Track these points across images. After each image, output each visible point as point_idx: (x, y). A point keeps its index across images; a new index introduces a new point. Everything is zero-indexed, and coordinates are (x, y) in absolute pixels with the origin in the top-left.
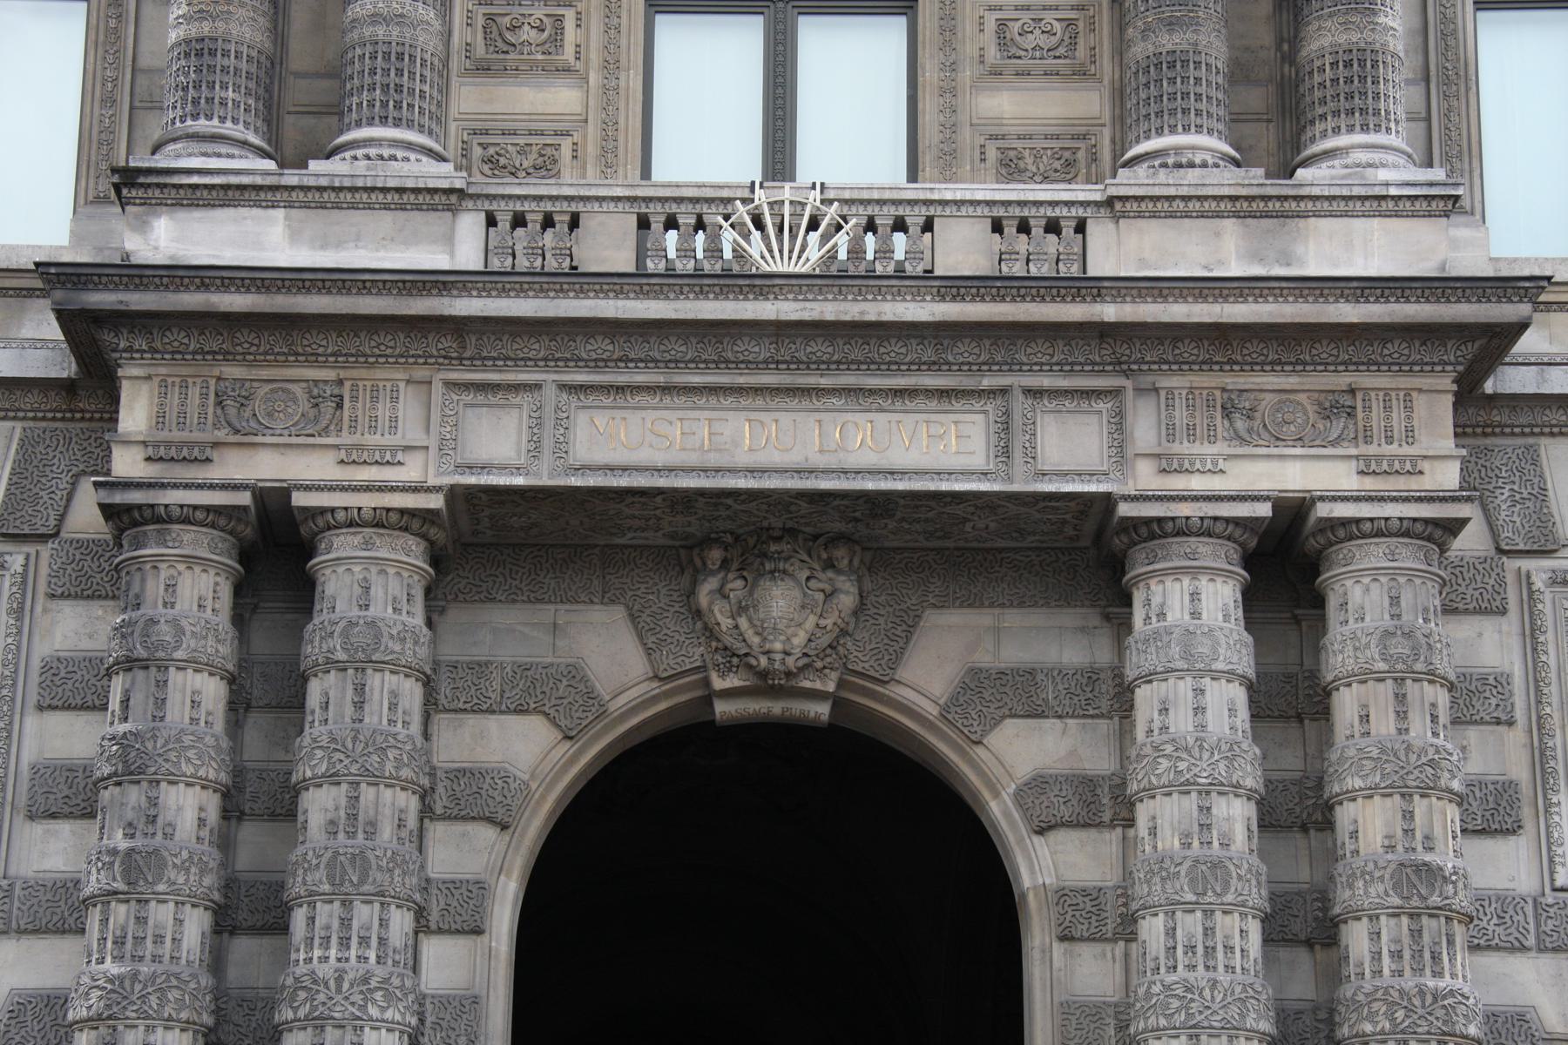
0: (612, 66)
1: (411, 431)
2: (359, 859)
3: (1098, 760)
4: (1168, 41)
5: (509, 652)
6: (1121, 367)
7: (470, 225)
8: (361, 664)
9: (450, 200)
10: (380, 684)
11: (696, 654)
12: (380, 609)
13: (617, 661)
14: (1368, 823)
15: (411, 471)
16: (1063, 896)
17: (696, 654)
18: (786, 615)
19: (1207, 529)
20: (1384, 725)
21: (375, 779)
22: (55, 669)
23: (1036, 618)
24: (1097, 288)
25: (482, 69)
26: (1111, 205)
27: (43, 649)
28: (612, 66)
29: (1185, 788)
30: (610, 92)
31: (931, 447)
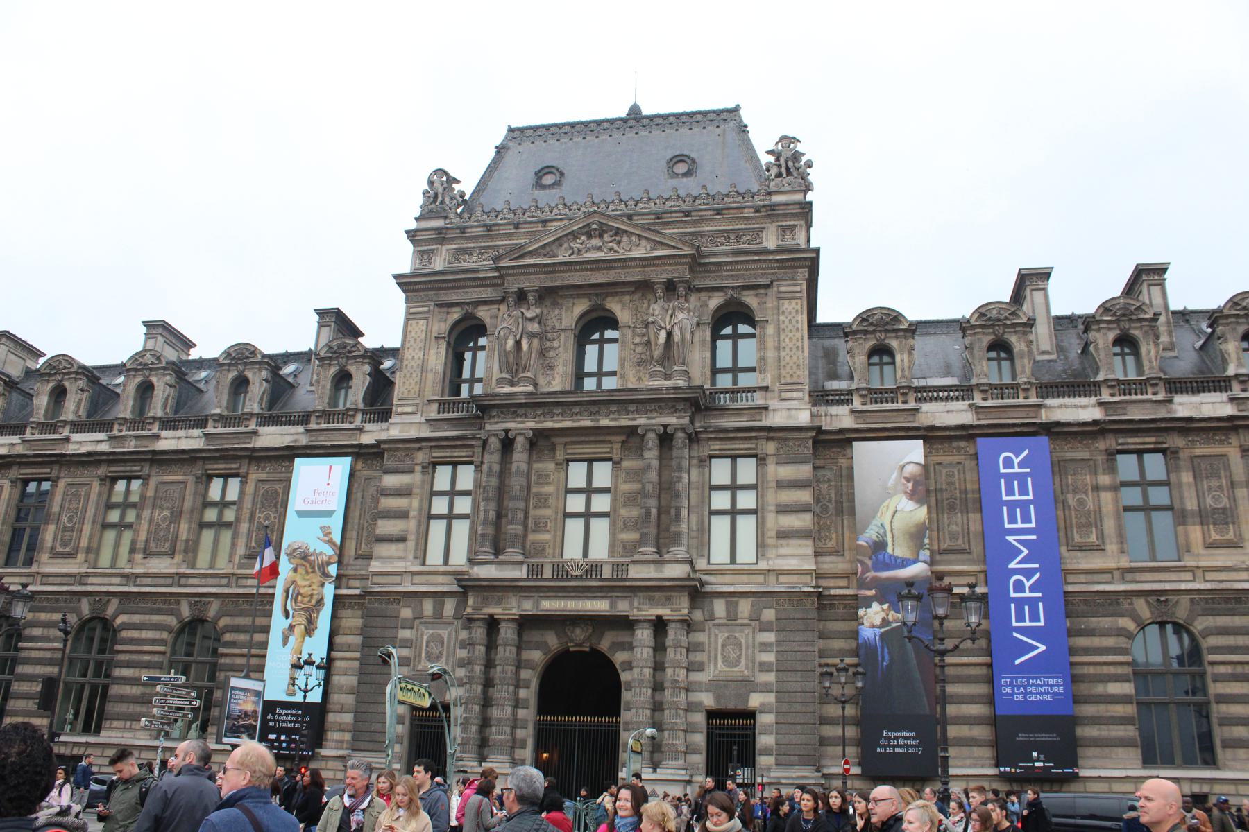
0: (555, 531)
1: (514, 604)
7: (525, 567)
8: (505, 645)
9: (522, 563)
12: (508, 635)
13: (553, 641)
15: (514, 611)
18: (579, 634)
19: (645, 621)
22: (463, 641)
24: (627, 580)
25: (534, 531)
26: (633, 562)
28: (555, 531)
30: (555, 536)
31: (599, 606)
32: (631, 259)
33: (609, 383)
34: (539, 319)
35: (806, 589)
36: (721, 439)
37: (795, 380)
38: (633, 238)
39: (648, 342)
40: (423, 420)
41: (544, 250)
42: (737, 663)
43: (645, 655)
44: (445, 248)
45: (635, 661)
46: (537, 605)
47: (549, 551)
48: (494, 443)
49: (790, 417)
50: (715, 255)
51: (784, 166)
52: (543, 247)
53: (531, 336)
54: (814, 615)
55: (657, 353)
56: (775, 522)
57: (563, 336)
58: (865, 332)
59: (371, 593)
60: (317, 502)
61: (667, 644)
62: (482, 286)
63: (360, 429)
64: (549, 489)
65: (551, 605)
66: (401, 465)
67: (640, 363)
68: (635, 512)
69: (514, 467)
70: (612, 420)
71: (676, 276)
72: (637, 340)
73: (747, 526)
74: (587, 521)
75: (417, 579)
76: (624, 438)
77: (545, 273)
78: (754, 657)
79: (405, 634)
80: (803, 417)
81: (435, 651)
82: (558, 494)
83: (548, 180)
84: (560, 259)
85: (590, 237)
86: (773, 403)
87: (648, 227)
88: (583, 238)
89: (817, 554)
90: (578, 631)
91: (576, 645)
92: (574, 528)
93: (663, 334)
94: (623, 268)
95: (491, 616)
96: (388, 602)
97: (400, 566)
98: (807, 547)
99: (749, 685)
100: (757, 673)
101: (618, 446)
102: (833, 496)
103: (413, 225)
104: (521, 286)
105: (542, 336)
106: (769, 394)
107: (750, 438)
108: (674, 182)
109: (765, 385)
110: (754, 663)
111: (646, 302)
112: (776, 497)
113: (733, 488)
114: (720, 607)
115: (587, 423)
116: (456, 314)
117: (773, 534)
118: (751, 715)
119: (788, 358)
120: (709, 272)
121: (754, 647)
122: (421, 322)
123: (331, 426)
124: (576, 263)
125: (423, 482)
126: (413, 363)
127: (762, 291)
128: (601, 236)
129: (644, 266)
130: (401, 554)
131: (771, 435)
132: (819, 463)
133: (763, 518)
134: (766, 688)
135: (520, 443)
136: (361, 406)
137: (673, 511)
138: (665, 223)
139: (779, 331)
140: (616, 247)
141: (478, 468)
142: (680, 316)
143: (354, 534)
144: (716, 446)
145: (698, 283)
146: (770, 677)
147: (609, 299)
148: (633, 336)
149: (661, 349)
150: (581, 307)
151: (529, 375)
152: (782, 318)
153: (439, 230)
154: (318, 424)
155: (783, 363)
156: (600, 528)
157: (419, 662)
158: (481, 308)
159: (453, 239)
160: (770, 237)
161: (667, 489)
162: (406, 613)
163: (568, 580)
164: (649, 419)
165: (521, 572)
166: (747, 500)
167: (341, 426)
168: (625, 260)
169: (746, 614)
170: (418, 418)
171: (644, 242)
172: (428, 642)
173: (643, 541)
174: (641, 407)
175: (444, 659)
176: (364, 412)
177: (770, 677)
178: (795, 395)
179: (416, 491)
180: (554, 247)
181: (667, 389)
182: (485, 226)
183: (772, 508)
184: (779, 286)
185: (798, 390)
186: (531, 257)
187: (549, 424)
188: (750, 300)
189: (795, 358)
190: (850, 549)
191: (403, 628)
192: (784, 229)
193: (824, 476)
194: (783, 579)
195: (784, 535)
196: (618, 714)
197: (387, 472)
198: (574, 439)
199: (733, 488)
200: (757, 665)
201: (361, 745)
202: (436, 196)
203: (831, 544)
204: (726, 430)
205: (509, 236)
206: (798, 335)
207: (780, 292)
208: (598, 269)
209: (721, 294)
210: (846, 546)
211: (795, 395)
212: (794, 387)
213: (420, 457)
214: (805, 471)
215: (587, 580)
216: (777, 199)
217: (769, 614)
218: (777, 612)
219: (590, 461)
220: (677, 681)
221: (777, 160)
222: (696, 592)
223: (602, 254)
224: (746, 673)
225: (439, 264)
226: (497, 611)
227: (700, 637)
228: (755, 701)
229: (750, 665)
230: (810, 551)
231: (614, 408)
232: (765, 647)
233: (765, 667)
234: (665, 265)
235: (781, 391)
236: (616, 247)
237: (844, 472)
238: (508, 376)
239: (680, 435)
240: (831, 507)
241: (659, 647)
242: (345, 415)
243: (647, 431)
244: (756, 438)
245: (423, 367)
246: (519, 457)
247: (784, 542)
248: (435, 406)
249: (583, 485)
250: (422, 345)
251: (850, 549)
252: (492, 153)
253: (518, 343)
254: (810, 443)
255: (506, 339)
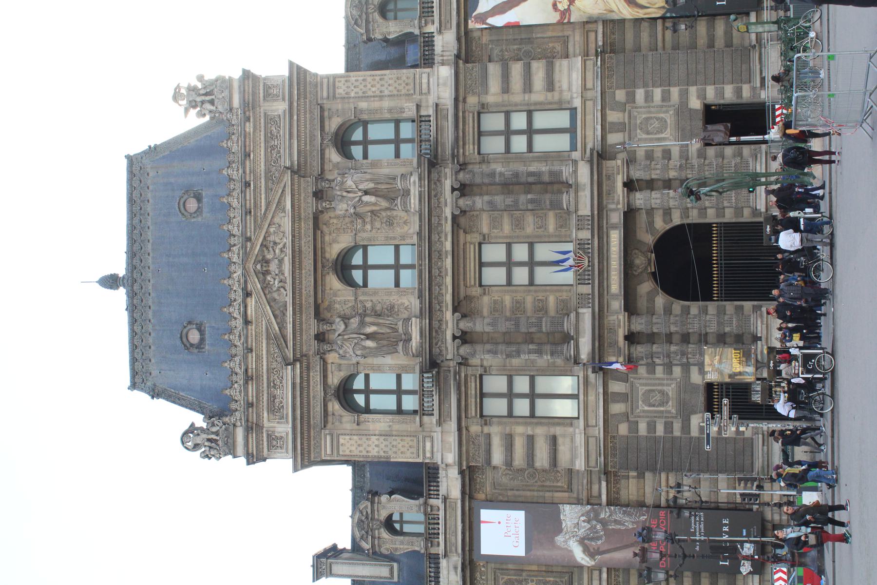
1: (615, 317)
2: (682, 322)
3: (661, 212)
4: (548, 202)
5: (645, 303)
6: (602, 211)
7: (581, 310)
8: (652, 323)
9: (577, 314)
10: (654, 321)
11: (645, 275)
12: (643, 321)
13: (646, 287)
14: (672, 174)
15: (621, 317)
16: (682, 218)
17: (645, 275)
18: (640, 261)
19: (628, 197)
20: (658, 172)
21: (669, 320)
22: (648, 372)
23: (638, 222)
24: (593, 214)
27: (645, 375)
28: (546, 291)
29: (668, 201)
30: (551, 291)
31: (615, 238)
32: (293, 230)
33: (407, 256)
34: (345, 319)
35: (599, 63)
36: (464, 144)
37: (411, 81)
38: (272, 230)
39: (372, 212)
40: (439, 429)
41: (280, 316)
42: (663, 121)
43: (658, 196)
44: (266, 424)
45: (666, 210)
46: (615, 296)
47: (564, 296)
48: (465, 350)
49: (445, 84)
50: (291, 155)
51: (203, 98)
52: (275, 316)
53: (362, 324)
54: (621, 56)
55: (384, 204)
56: (539, 94)
57: (361, 298)
58: (367, 22)
59: (606, 465)
60: (517, 533)
61: (648, 178)
62: (308, 381)
63: (445, 499)
64: (507, 300)
65: (615, 284)
66: (483, 447)
67: (390, 222)
68: (530, 219)
69: (488, 329)
70: (446, 239)
71: (310, 190)
72: (368, 227)
73: (541, 120)
74: (539, 264)
75: (592, 422)
76: (461, 232)
77: (301, 314)
78: (657, 106)
79: (643, 428)
80: (445, 72)
81: (658, 397)
82: (513, 291)
83: (194, 337)
84: (289, 300)
85: (267, 272)
86: (432, 99)
87: (258, 227)
88: (269, 278)
89: (567, 57)
90: (637, 262)
91: (649, 264)
92: (544, 275)
93: (366, 198)
94: (300, 239)
95: (626, 338)
96: (614, 448)
97: (580, 439)
98: (562, 65)
99: (683, 109)
100: (672, 103)
101: (469, 237)
102: (515, 47)
103: (243, 460)
104: (313, 337)
105: (363, 315)
106: (423, 104)
107: (464, 118)
108: (205, 210)
109: (415, 107)
110: (662, 107)
111: (332, 221)
112: (517, 96)
113: (508, 133)
114: (614, 138)
115: (448, 262)
116: (335, 406)
117: (549, 95)
118: (707, 108)
119: (390, 88)
120: (306, 163)
121: (649, 107)
122: (341, 441)
123: (441, 531)
124: (293, 283)
125: (499, 423)
126: (382, 446)
127: (326, 114)
128: (267, 262)
129: (300, 219)
130: (568, 440)
131: (461, 99)
132: (486, 58)
133: (536, 104)
134: (684, 95)
135: (465, 325)
136: (421, 500)
137: (531, 179)
138: (255, 206)
139: (365, 97)
140: (280, 246)
141: (486, 371)
142: (350, 183)
143: (548, 494)
144: (470, 148)
145: (317, 170)
146: (675, 91)
147: (327, 255)
148: (364, 231)
149: (379, 199)
150: (334, 282)
151: (401, 323)
152: (353, 95)
153: (248, 430)
154: (438, 545)
155: (395, 93)
156: (544, 252)
157: (669, 412)
158: (330, 381)
159: (258, 416)
160: (274, 108)
161: (510, 185)
162: (623, 429)
163: (593, 266)
164: (446, 205)
165: (586, 314)
166: (519, 121)
167: (441, 521)
168: (293, 236)
169: (620, 115)
170: (437, 436)
171: (276, 220)
172: (650, 405)
173: (556, 205)
174: (434, 213)
175: (665, 388)
176: (429, 496)
177: (675, 91)
178: (425, 81)
179: (508, 431)
180: (276, 307)
181: (420, 186)
182: (246, 382)
183: (527, 96)
184: (322, 98)
185: (421, 78)
186: (286, 328)
187: (449, 298)
188: (333, 125)
189: (391, 82)
190: (563, 31)
191: (637, 431)
192: (267, 96)
193: (498, 55)
194: (589, 85)
195: (550, 85)
196: (709, 226)
197: (488, 461)
198: (461, 277)
199: (508, 133)
200: (664, 104)
201: (747, 463)
202: (209, 440)
203: (558, 47)
204: (457, 139)
205: (259, 358)
206: (369, 79)
207: (328, 98)
208: (300, 263)
209: (327, 151)
210: (560, 34)
211: (425, 81)
212: (417, 81)
213: (475, 429)
214: (494, 69)
215: (591, 268)
216: (236, 102)
217: (620, 95)
218: (618, 88)
219: (481, 265)
220: (681, 166)
221: (194, 107)
222: (601, 156)
223: (286, 259)
224: (671, 112)
225: (284, 429)
226: (621, 333)
227: (641, 154)
228: (695, 104)
229: (664, 109)
230: (565, 62)
231: (435, 237)
232: (648, 97)
233: (666, 97)
234: (299, 200)
235: (421, 93)
236: (280, 246)
237: (494, 38)
238: (401, 344)
239: (461, 176)
240: (528, 47)
241: (650, 185)
242: (431, 520)
243: (457, 206)
244: (464, 112)
245: (386, 435)
246: (479, 326)
247: (557, 85)
248: (426, 419)
249: (503, 271)
250: (364, 438)
251: (563, 31)
252: (161, 402)
253: (369, 336)
254: (470, 65)
255: (365, 348)
